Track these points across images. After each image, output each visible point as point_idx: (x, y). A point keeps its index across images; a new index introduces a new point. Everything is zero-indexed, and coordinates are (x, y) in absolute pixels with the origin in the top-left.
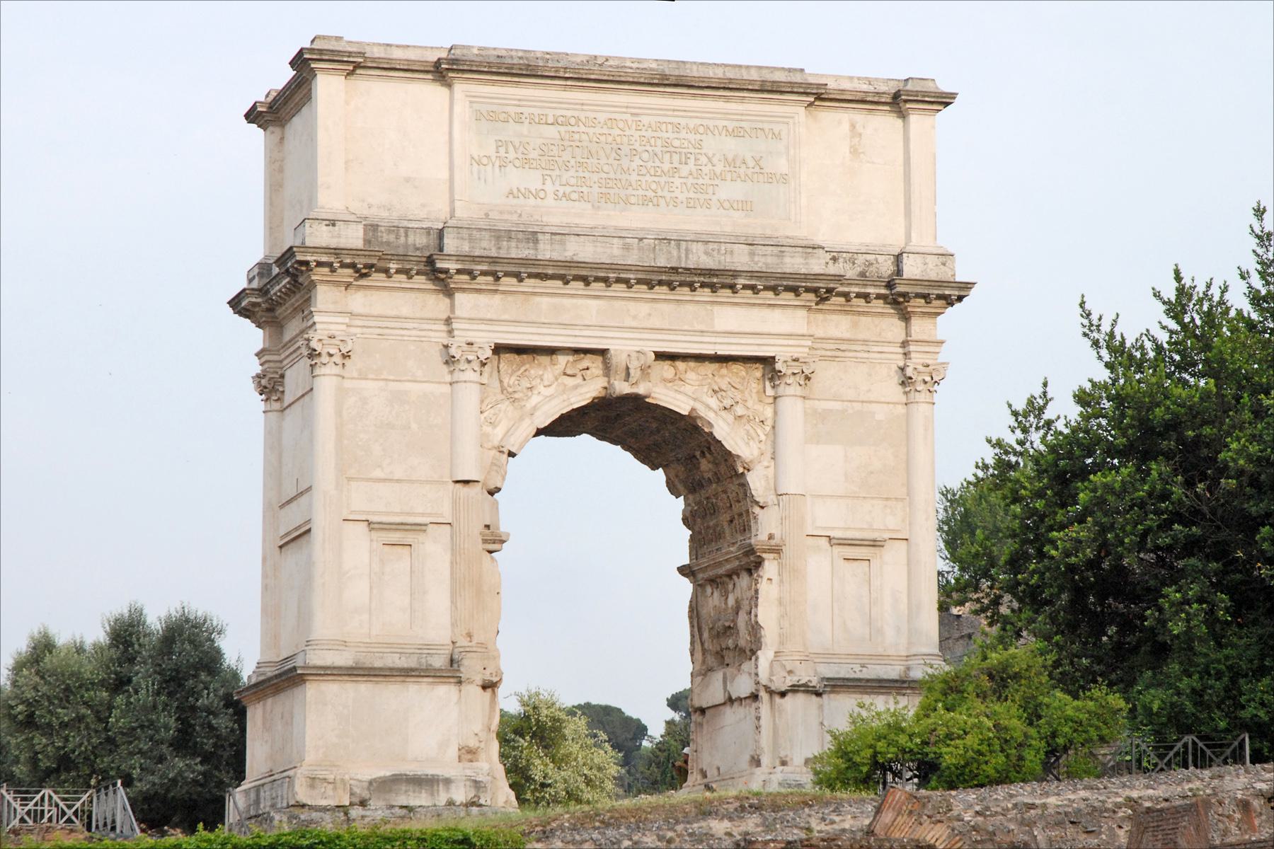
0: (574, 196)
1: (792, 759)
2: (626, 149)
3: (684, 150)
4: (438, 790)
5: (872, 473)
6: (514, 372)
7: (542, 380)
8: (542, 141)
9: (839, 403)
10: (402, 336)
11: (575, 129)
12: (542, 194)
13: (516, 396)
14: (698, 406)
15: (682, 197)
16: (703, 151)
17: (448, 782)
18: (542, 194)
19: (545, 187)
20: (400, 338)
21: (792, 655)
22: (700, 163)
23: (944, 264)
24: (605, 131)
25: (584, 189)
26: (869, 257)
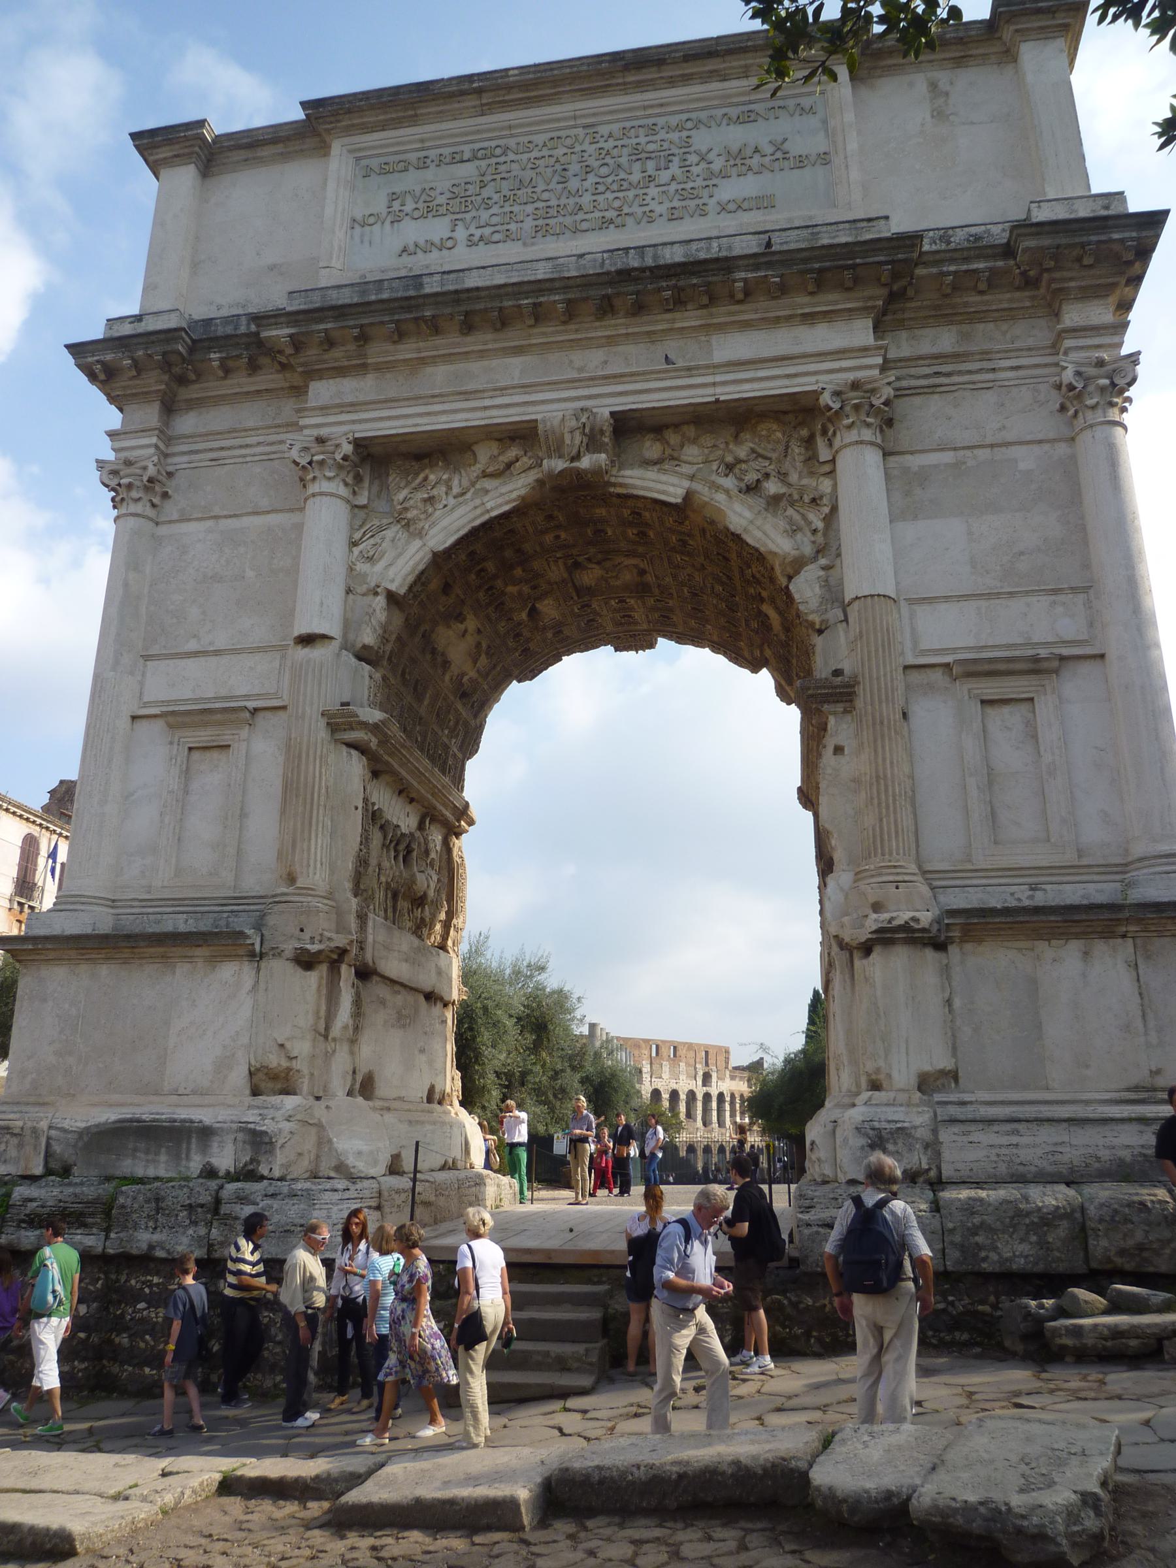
0: (496, 237)
1: (889, 1076)
2: (574, 168)
3: (662, 154)
4: (188, 1150)
5: (1022, 553)
6: (408, 484)
7: (450, 488)
8: (453, 182)
9: (952, 453)
10: (244, 456)
11: (502, 159)
12: (450, 244)
13: (409, 515)
14: (697, 486)
15: (659, 209)
16: (691, 149)
17: (206, 1133)
18: (450, 244)
19: (453, 235)
20: (241, 460)
21: (880, 875)
22: (687, 163)
23: (1107, 208)
24: (545, 152)
25: (513, 227)
26: (973, 230)
